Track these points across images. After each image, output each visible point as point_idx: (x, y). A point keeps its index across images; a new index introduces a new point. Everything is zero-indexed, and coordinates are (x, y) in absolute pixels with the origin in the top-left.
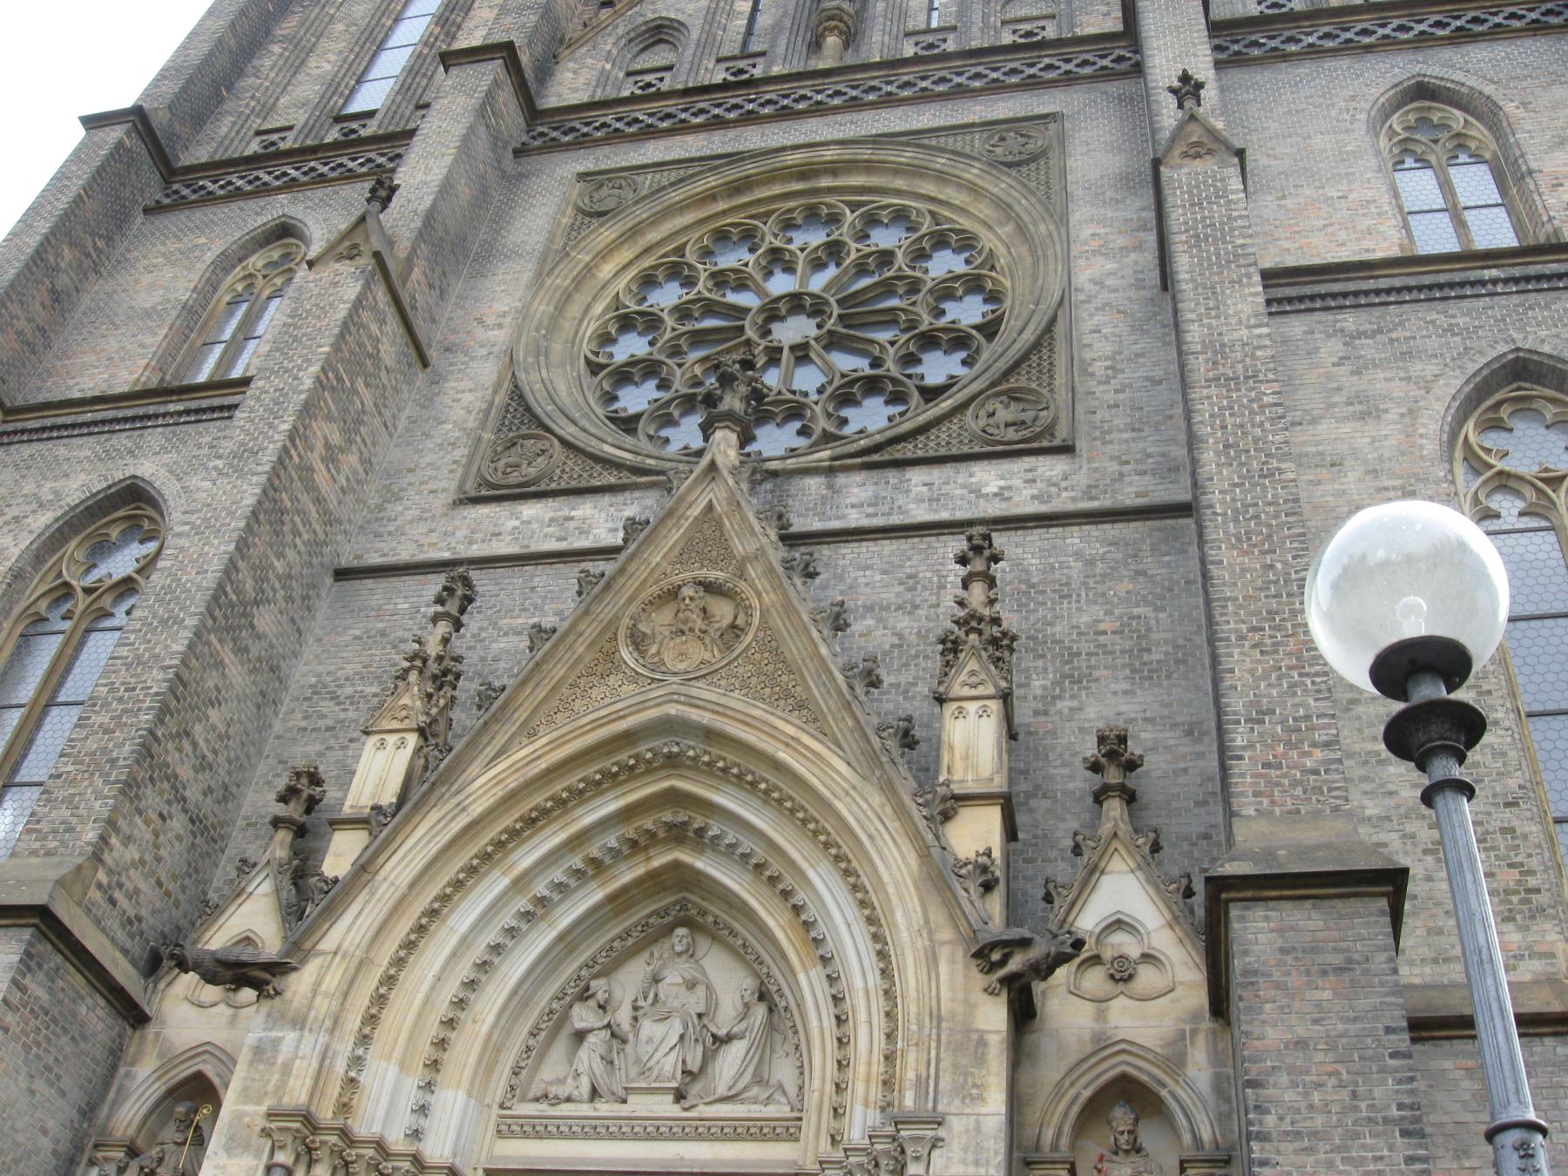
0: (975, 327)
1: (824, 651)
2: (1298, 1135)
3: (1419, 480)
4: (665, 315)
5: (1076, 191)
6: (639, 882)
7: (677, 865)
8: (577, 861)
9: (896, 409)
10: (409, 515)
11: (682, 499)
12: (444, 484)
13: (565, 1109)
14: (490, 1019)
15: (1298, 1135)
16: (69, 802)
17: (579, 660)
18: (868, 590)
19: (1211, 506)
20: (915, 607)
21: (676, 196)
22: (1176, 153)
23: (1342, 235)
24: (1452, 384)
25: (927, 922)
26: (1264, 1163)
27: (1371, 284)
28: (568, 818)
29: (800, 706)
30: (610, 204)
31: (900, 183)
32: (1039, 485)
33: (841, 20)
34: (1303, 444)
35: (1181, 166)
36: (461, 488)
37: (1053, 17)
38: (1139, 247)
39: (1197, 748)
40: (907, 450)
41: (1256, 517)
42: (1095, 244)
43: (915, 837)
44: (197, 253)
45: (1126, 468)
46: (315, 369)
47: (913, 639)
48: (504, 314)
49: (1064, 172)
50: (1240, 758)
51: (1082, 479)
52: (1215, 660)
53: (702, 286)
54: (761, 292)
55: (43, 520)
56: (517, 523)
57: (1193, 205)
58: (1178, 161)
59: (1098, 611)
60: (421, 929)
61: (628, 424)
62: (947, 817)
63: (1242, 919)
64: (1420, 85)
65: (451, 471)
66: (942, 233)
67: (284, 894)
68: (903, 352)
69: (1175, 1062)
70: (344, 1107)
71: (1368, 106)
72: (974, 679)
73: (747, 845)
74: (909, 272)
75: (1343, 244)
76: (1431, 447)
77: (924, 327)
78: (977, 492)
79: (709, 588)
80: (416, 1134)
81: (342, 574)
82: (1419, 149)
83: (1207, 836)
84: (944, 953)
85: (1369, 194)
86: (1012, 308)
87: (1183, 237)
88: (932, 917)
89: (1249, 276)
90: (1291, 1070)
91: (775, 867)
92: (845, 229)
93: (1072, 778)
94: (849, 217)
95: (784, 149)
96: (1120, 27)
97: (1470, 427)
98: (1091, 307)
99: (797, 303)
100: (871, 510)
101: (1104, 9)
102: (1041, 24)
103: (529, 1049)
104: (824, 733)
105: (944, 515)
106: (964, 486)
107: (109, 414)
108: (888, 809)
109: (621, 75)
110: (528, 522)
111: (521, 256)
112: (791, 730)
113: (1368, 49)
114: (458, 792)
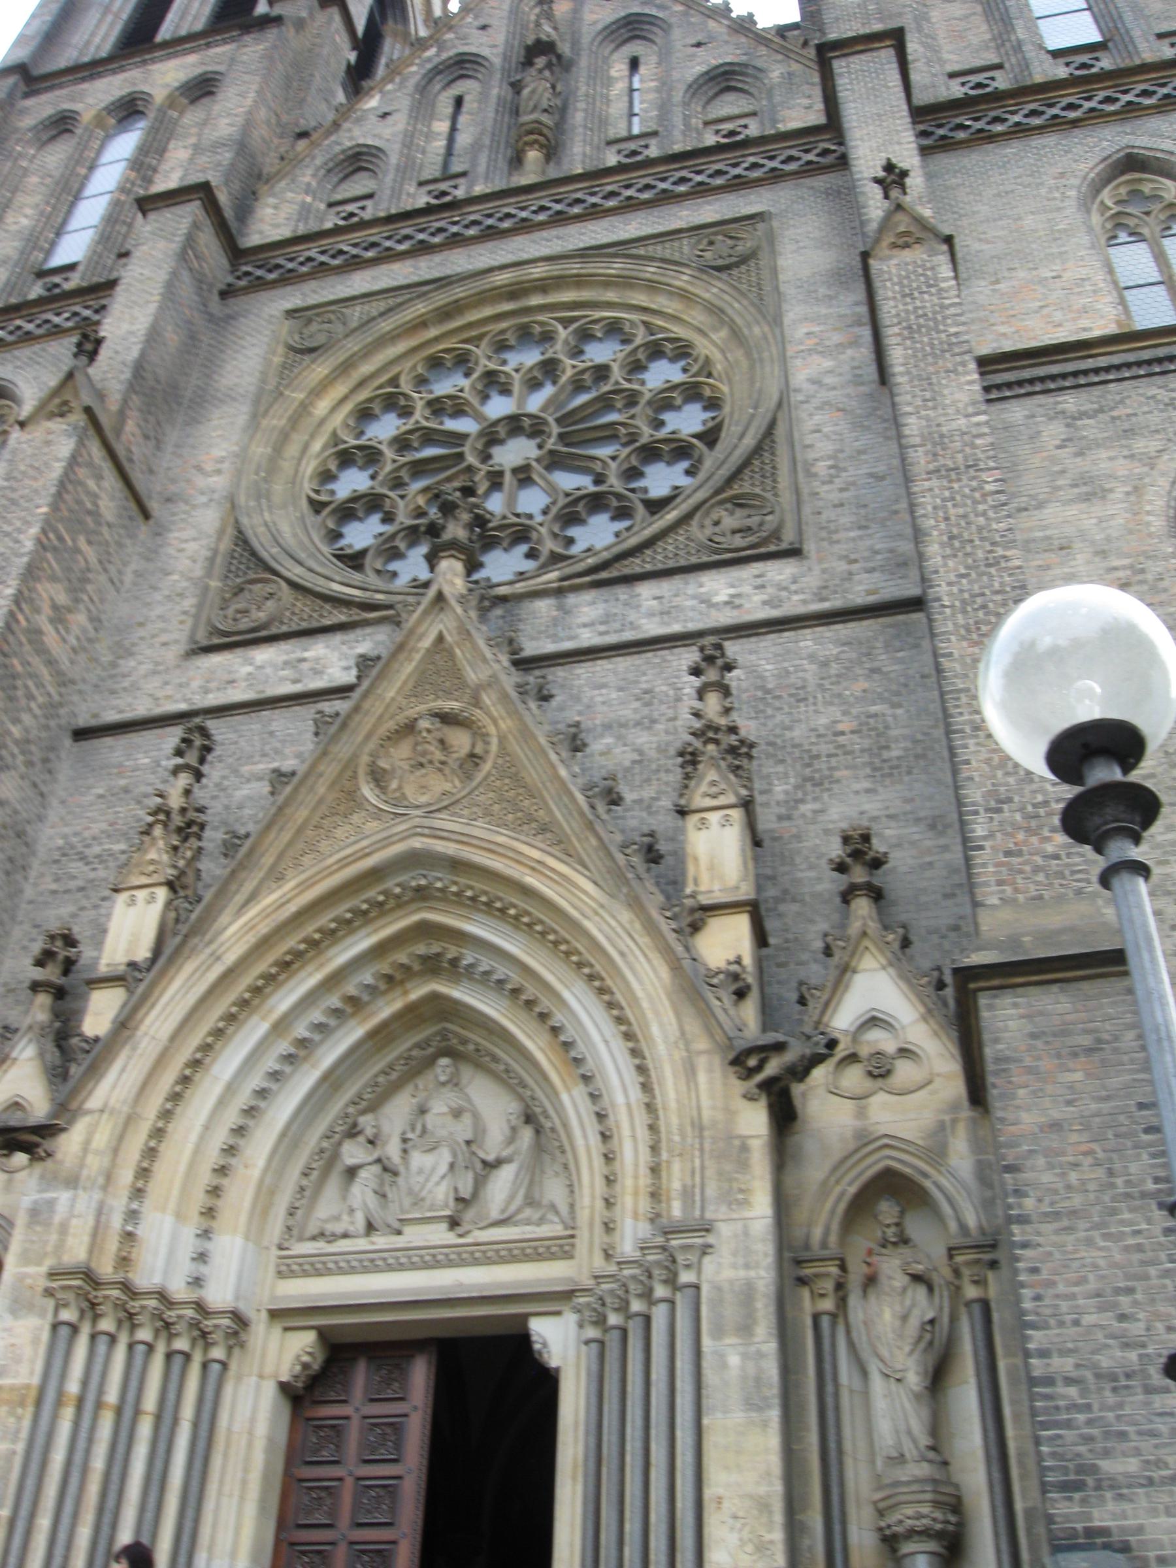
0: (694, 436)
1: (563, 772)
2: (1056, 1215)
3: (1148, 558)
4: (384, 448)
5: (788, 290)
6: (398, 1016)
7: (435, 997)
8: (334, 1001)
9: (621, 525)
10: (144, 669)
11: (412, 632)
12: (175, 636)
14: (261, 1163)
15: (1056, 1215)
17: (321, 801)
18: (605, 708)
19: (938, 599)
20: (654, 721)
21: (386, 325)
22: (884, 244)
23: (1058, 316)
25: (683, 1034)
26: (1025, 1245)
27: (1090, 363)
28: (322, 959)
29: (543, 829)
30: (321, 339)
31: (611, 296)
32: (770, 590)
33: (541, 134)
34: (1031, 529)
35: (890, 258)
36: (192, 639)
37: (754, 114)
38: (855, 343)
39: (942, 841)
40: (635, 565)
41: (984, 607)
42: (810, 343)
43: (666, 951)
45: (855, 567)
46: (34, 530)
47: (653, 754)
48: (221, 460)
49: (774, 271)
50: (981, 848)
51: (812, 581)
52: (952, 754)
53: (420, 415)
54: (478, 417)
56: (250, 669)
57: (904, 296)
58: (887, 252)
59: (835, 712)
60: (185, 1080)
61: (354, 561)
62: (695, 928)
63: (991, 1007)
64: (1129, 156)
65: (181, 622)
66: (656, 343)
67: (48, 1057)
68: (626, 466)
69: (937, 1152)
70: (124, 1261)
71: (1076, 182)
72: (714, 790)
73: (502, 971)
74: (627, 385)
75: (1060, 325)
77: (644, 440)
78: (707, 601)
79: (446, 719)
80: (197, 1282)
81: (82, 734)
82: (1132, 222)
83: (956, 928)
84: (702, 1062)
85: (1084, 272)
86: (732, 414)
87: (896, 330)
88: (687, 1028)
89: (963, 364)
90: (1048, 1153)
91: (531, 991)
92: (559, 346)
93: (819, 879)
94: (563, 333)
95: (491, 270)
96: (822, 120)
99: (515, 425)
100: (602, 628)
101: (806, 102)
102: (743, 122)
103: (302, 1189)
104: (569, 855)
105: (676, 628)
106: (694, 597)
108: (638, 926)
109: (322, 206)
110: (261, 667)
111: (234, 399)
112: (536, 854)
113: (1075, 123)
114: (211, 942)
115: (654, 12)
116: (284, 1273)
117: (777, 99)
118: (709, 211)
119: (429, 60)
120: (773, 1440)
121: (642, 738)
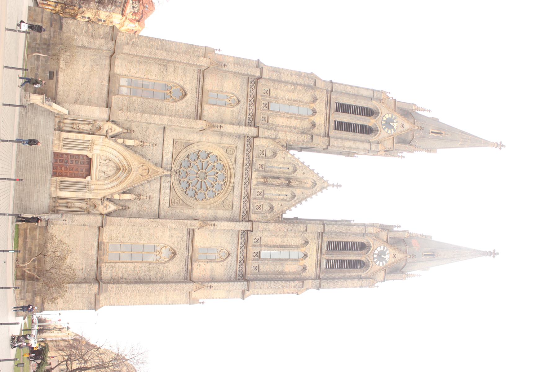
24: (173, 246)
31: (226, 189)
35: (198, 222)
38: (202, 217)
40: (172, 190)
46: (185, 126)
48: (208, 140)
49: (220, 210)
51: (165, 208)
55: (182, 84)
69: (97, 210)
70: (96, 145)
77: (197, 192)
97: (168, 247)
101: (259, 218)
102: (261, 209)
107: (200, 87)
115: (294, 199)
116: (97, 155)
118: (236, 202)
119: (298, 164)
121: (148, 190)
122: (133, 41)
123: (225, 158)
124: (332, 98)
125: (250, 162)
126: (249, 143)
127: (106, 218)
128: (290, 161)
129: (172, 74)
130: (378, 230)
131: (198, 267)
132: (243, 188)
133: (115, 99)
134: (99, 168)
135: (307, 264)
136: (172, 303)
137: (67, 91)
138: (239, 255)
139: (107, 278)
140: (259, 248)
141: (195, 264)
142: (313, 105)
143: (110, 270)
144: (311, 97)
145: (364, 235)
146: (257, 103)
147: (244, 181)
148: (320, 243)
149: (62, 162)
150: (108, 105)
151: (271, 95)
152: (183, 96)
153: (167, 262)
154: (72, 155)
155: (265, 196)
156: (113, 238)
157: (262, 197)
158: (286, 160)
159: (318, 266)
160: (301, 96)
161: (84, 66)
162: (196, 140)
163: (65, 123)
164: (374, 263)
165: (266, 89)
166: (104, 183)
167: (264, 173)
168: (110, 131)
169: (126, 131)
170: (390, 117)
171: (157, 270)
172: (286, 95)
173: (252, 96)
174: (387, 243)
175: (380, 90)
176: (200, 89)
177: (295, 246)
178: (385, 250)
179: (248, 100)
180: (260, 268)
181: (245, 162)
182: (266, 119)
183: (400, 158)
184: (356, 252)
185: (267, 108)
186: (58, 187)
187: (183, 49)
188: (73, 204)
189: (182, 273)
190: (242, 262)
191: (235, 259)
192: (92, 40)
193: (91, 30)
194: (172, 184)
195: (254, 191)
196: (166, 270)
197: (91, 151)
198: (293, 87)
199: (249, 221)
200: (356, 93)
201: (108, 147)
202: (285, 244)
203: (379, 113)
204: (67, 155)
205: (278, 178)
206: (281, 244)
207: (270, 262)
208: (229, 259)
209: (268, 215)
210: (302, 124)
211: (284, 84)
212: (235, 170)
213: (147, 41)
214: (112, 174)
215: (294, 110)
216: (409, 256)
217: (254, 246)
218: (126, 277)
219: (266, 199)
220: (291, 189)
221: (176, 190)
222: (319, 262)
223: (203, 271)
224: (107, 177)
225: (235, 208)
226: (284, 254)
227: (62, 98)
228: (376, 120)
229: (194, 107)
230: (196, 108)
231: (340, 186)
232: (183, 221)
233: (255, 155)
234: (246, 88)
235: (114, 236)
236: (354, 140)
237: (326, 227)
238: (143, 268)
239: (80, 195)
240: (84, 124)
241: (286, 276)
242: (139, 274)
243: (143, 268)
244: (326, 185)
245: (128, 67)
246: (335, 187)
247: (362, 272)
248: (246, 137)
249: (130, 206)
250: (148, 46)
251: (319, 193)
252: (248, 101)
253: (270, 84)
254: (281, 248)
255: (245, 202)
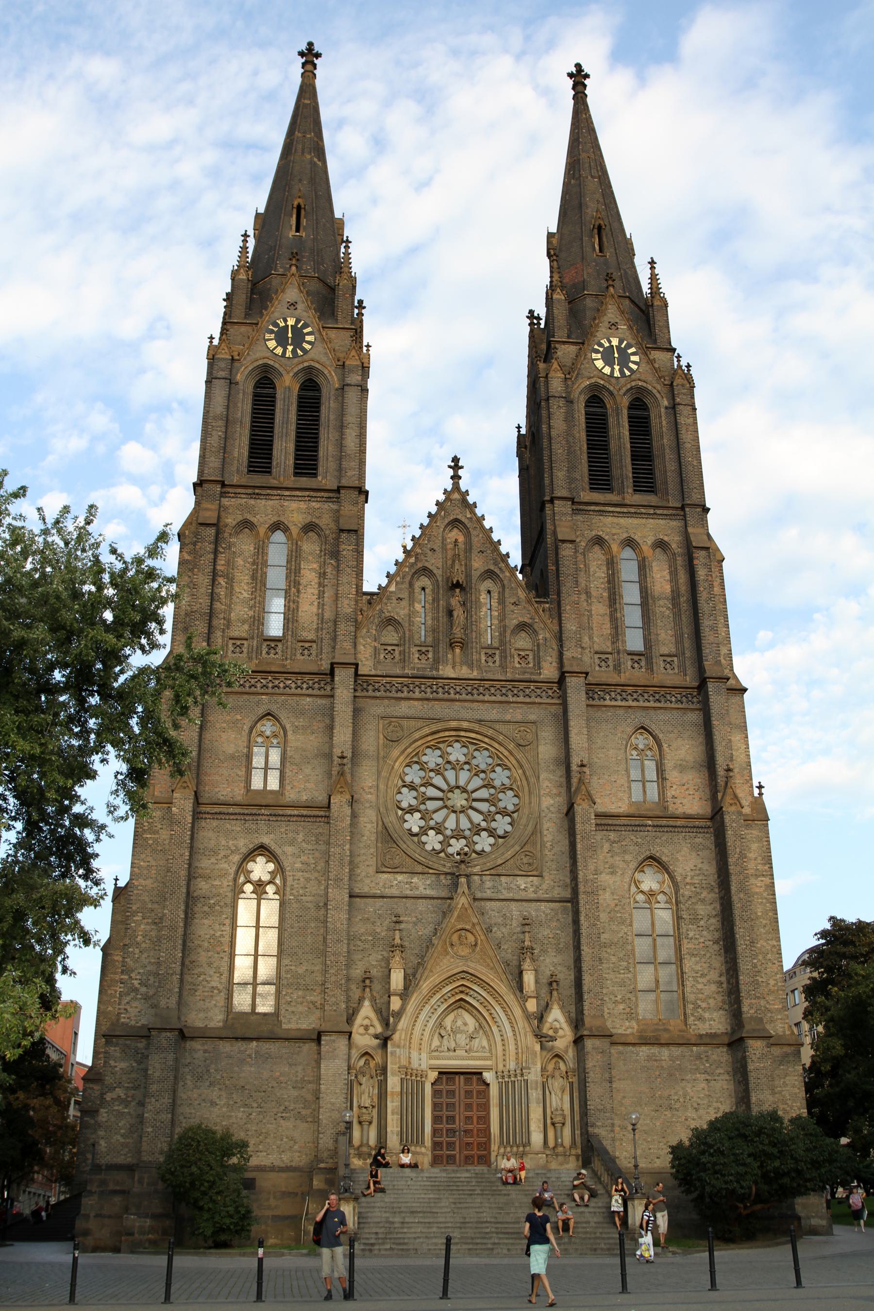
10: (363, 874)
12: (371, 863)
13: (442, 1054)
16: (334, 995)
24: (633, 865)
29: (492, 969)
31: (486, 740)
35: (579, 805)
38: (559, 795)
40: (500, 870)
44: (239, 725)
46: (348, 846)
48: (370, 787)
51: (545, 886)
55: (236, 858)
69: (566, 1052)
70: (410, 1063)
76: (626, 886)
91: (486, 1004)
98: (546, 819)
102: (527, 653)
105: (510, 895)
107: (242, 811)
115: (498, 571)
116: (431, 1058)
117: (541, 654)
119: (412, 565)
120: (541, 1109)
122: (139, 986)
123: (411, 745)
124: (238, 483)
125: (417, 683)
126: (370, 687)
127: (590, 1030)
128: (406, 585)
129: (215, 883)
130: (555, 365)
131: (678, 801)
132: (481, 697)
133: (289, 1022)
134: (460, 1053)
135: (650, 540)
136: (768, 860)
137: (279, 1142)
138: (641, 704)
139: (723, 1020)
140: (621, 656)
141: (672, 809)
142: (262, 530)
143: (703, 1014)
144: (241, 536)
145: (569, 402)
146: (268, 669)
147: (464, 696)
148: (597, 508)
149: (454, 1143)
150: (318, 1038)
151: (244, 635)
152: (267, 853)
153: (672, 878)
154: (436, 1119)
155: (496, 645)
156: (628, 1010)
157: (497, 652)
158: (405, 595)
159: (652, 511)
160: (240, 561)
161: (213, 1104)
162: (374, 819)
163: (362, 1142)
164: (633, 377)
165: (231, 648)
166: (498, 1039)
167: (441, 649)
168: (372, 1031)
169: (368, 990)
170: (273, 336)
171: (694, 900)
172: (241, 597)
173: (253, 681)
174: (583, 343)
175: (205, 363)
176: (246, 812)
177: (608, 569)
178: (601, 349)
179: (262, 691)
180: (666, 652)
181: (417, 695)
182: (307, 645)
183: (363, 311)
184: (611, 420)
185: (280, 645)
186: (521, 1149)
187: (149, 859)
188: (557, 1110)
189: (697, 840)
190: (657, 696)
191: (652, 712)
192: (154, 1088)
193: (120, 1092)
194: (488, 873)
195: (486, 671)
196: (692, 878)
197: (423, 1075)
198: (222, 581)
199: (561, 681)
200: (221, 423)
201: (412, 1033)
202: (606, 594)
203: (266, 365)
204: (435, 1132)
205: (450, 613)
206: (607, 603)
207: (653, 629)
208: (653, 727)
209: (541, 637)
210: (311, 558)
211: (214, 603)
212: (439, 720)
213: (137, 951)
214: (474, 1020)
215: (276, 577)
216: (611, 289)
217: (617, 668)
218: (717, 975)
219: (502, 642)
220: (474, 581)
221: (500, 861)
222: (643, 511)
223: (688, 789)
224: (481, 1032)
225: (532, 718)
226: (631, 594)
227: (298, 1154)
228: (284, 373)
229: (292, 826)
230: (294, 819)
231: (456, 460)
232: (578, 841)
233: (398, 671)
234: (235, 697)
235: (621, 1007)
236: (341, 427)
237: (559, 495)
238: (691, 934)
239: (535, 1095)
240: (360, 1096)
241: (684, 588)
242: (707, 943)
243: (691, 934)
244: (456, 496)
245: (206, 994)
246: (461, 472)
247: (659, 405)
248: (357, 694)
249: (549, 973)
250: (147, 946)
251: (479, 512)
252: (266, 691)
253: (218, 638)
254: (617, 601)
255: (515, 692)
